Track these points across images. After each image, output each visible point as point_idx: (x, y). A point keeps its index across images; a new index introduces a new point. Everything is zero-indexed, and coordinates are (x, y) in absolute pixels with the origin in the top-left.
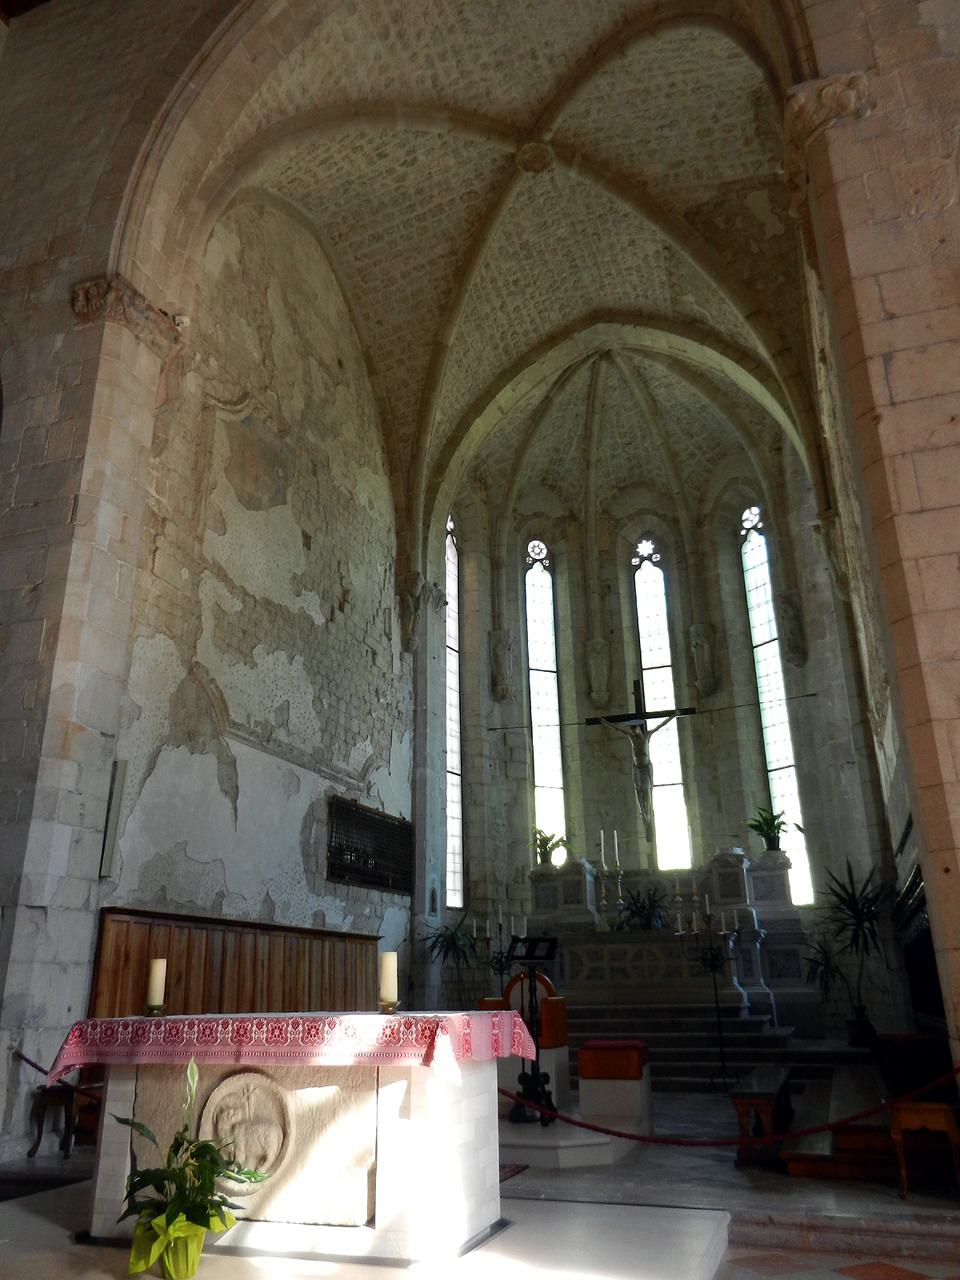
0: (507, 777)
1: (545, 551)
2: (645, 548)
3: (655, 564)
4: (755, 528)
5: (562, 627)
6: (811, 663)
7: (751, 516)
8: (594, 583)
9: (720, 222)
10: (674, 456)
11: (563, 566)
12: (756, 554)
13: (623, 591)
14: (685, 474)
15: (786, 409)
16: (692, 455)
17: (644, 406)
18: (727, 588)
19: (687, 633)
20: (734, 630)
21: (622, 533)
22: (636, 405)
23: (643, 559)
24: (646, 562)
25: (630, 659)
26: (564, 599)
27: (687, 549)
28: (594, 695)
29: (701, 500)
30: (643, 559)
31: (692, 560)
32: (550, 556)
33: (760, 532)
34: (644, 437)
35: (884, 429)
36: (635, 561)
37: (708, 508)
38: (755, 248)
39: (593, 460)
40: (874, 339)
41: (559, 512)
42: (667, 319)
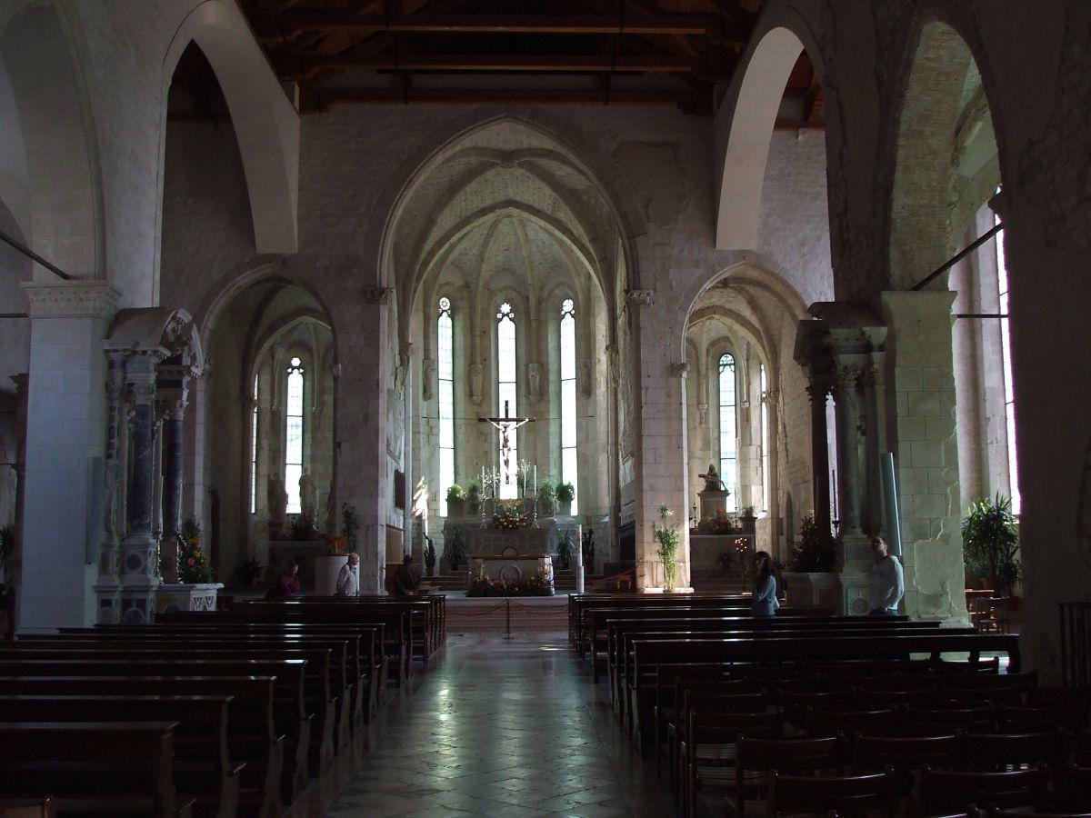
0: (429, 443)
1: (449, 304)
2: (506, 308)
3: (511, 319)
4: (570, 312)
5: (458, 353)
6: (591, 399)
7: (568, 305)
8: (478, 332)
9: (585, 198)
10: (532, 262)
11: (459, 317)
12: (568, 327)
13: (492, 333)
14: (535, 273)
15: (600, 281)
16: (541, 264)
17: (521, 239)
18: (551, 345)
19: (527, 366)
20: (552, 368)
21: (495, 299)
22: (516, 234)
23: (504, 315)
24: (506, 317)
25: (493, 377)
26: (459, 338)
27: (533, 316)
28: (474, 398)
29: (542, 288)
30: (504, 315)
31: (534, 324)
32: (452, 308)
33: (573, 316)
34: (516, 250)
35: (643, 410)
36: (499, 316)
37: (545, 294)
38: (598, 212)
39: (486, 258)
40: (645, 382)
41: (459, 282)
42: (547, 215)
